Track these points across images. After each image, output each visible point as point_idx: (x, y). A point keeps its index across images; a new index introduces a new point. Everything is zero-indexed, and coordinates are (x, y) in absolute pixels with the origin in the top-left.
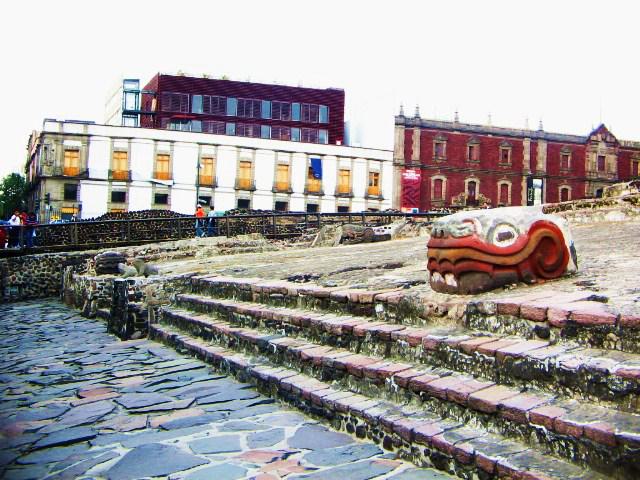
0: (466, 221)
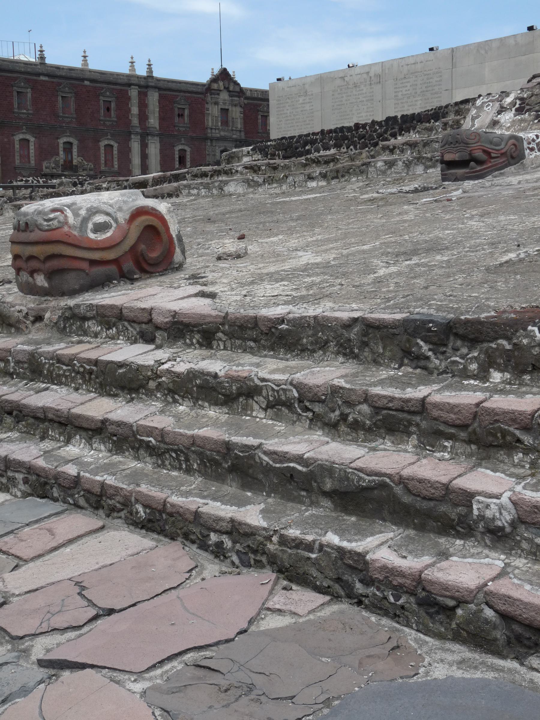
0: (54, 210)
